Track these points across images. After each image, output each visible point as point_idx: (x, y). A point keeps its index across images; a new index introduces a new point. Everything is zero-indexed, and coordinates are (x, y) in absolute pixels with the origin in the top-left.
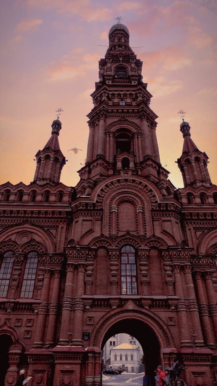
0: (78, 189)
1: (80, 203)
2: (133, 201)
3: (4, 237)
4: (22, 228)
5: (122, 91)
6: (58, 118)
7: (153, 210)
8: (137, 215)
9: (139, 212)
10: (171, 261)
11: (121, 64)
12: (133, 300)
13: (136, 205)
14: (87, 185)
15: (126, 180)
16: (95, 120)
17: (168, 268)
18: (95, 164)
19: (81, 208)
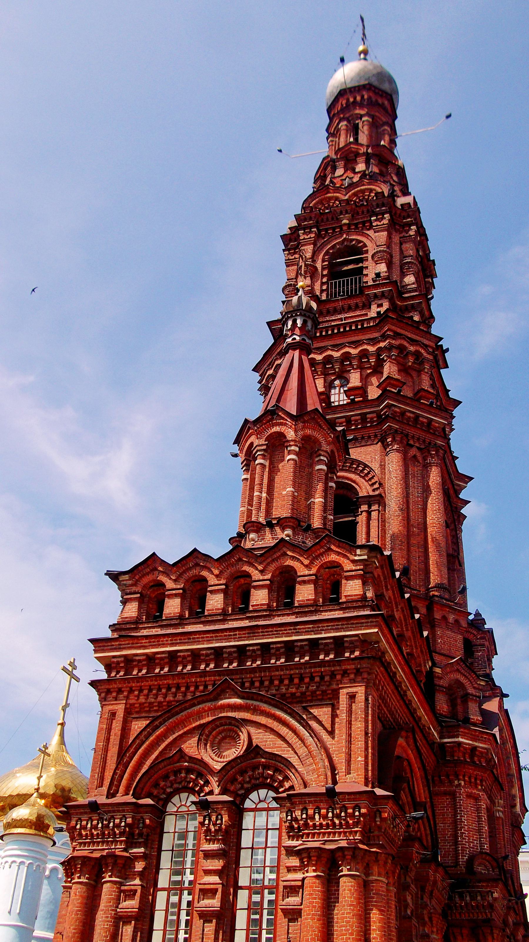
0: (441, 678)
16: (413, 437)
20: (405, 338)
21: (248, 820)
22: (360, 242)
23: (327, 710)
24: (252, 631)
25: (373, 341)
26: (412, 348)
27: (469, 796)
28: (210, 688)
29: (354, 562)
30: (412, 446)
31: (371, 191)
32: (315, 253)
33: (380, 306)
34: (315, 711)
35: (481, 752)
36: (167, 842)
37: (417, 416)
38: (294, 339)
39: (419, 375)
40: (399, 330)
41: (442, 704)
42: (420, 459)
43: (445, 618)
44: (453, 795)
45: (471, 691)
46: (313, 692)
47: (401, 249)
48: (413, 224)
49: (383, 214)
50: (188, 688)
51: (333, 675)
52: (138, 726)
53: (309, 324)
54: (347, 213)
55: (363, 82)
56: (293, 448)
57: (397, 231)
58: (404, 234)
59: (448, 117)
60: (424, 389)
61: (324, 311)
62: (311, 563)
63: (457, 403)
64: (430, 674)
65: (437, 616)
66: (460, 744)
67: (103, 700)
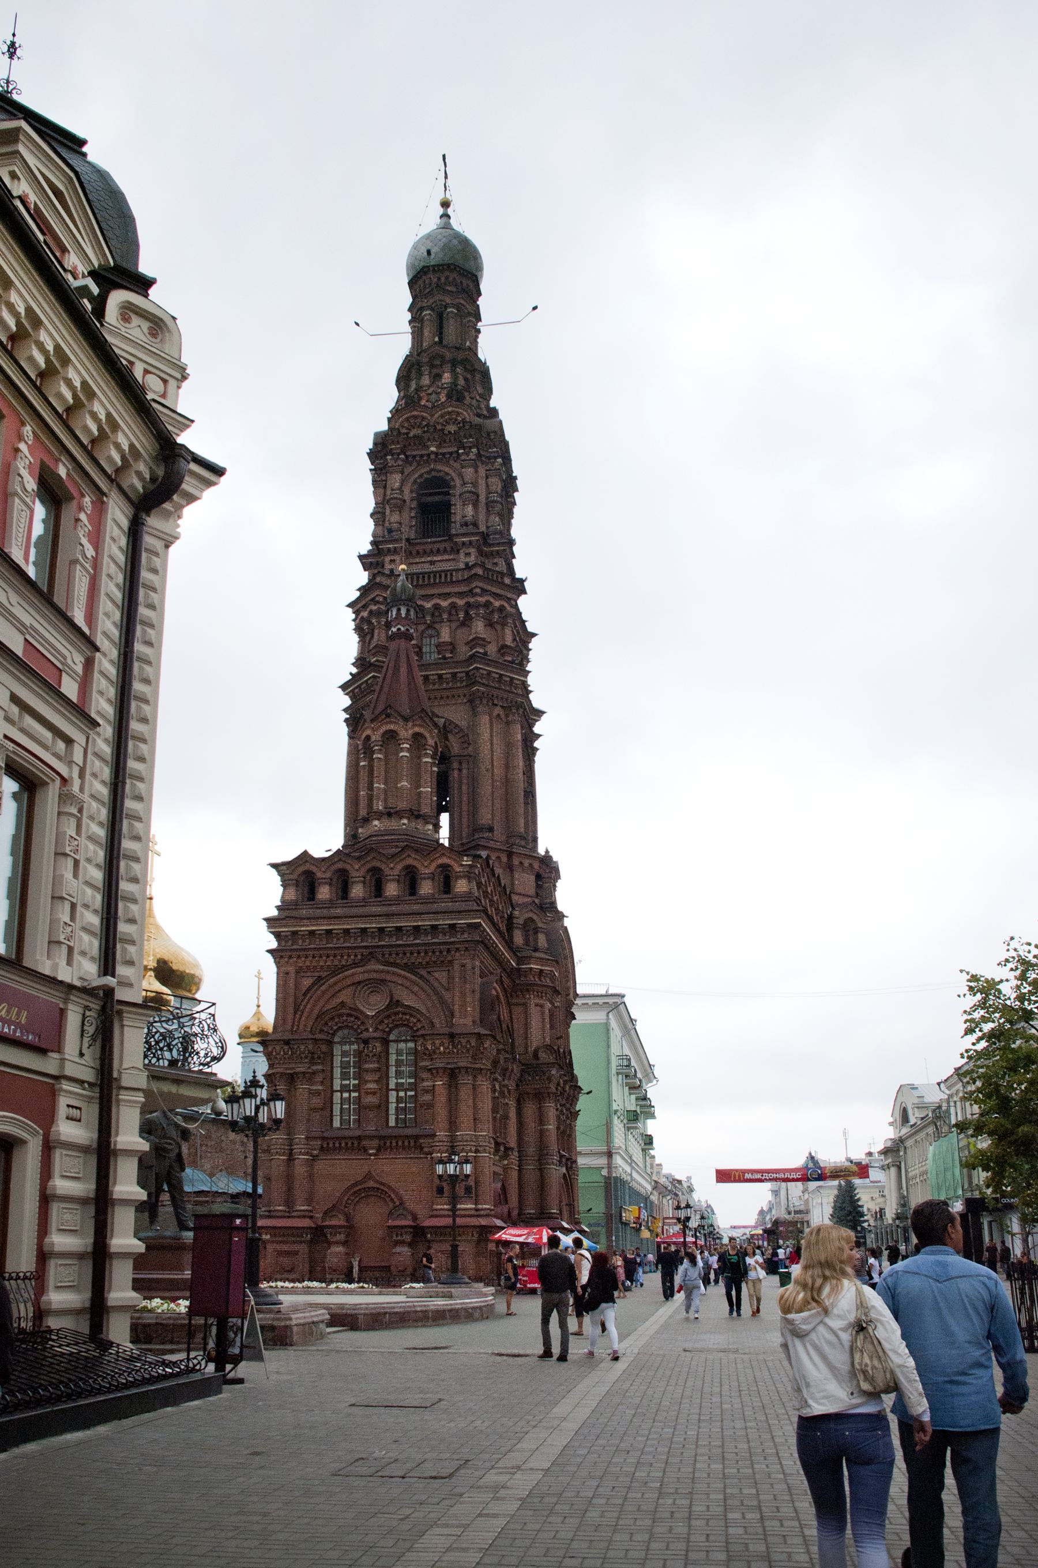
21: (393, 1048)
22: (448, 474)
23: (445, 974)
24: (389, 916)
25: (461, 595)
26: (497, 604)
28: (359, 957)
29: (462, 865)
31: (458, 414)
32: (403, 482)
33: (468, 554)
34: (436, 975)
36: (337, 1061)
37: (501, 675)
38: (399, 629)
39: (503, 629)
41: (518, 938)
42: (503, 716)
44: (525, 1005)
45: (540, 925)
46: (434, 962)
47: (487, 486)
48: (499, 457)
49: (470, 448)
50: (342, 956)
51: (449, 951)
52: (307, 982)
53: (412, 613)
54: (434, 440)
55: (447, 260)
56: (405, 745)
57: (483, 463)
58: (490, 466)
59: (535, 308)
60: (507, 646)
61: (414, 552)
63: (534, 635)
64: (510, 917)
65: (516, 861)
67: (277, 963)
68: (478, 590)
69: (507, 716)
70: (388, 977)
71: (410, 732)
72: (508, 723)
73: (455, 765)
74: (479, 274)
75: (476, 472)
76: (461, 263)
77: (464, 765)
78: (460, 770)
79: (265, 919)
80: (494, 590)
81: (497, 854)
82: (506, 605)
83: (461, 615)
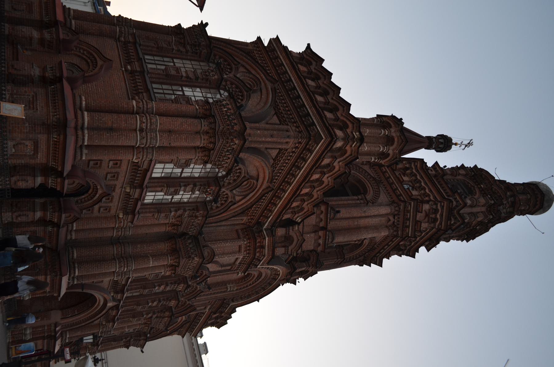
1: (264, 256)
2: (245, 281)
3: (257, 164)
4: (263, 183)
5: (421, 239)
6: (456, 144)
7: (225, 299)
8: (226, 285)
9: (227, 288)
10: (157, 317)
11: (470, 227)
12: (118, 305)
13: (239, 283)
14: (290, 250)
15: (276, 280)
16: (399, 218)
17: (150, 315)
18: (321, 241)
19: (258, 255)
20: (442, 212)
26: (438, 216)
27: (240, 247)
29: (352, 133)
30: (394, 218)
35: (262, 252)
40: (445, 208)
41: (281, 232)
43: (320, 237)
45: (290, 248)
49: (493, 200)
51: (295, 122)
62: (344, 117)
65: (321, 233)
66: (265, 238)
68: (443, 204)
69: (390, 226)
70: (264, 91)
71: (394, 135)
72: (387, 227)
73: (360, 197)
74: (541, 210)
75: (483, 206)
76: (545, 199)
77: (362, 201)
78: (358, 200)
79: (277, 36)
80: (444, 214)
81: (323, 219)
82: (438, 222)
83: (427, 198)
